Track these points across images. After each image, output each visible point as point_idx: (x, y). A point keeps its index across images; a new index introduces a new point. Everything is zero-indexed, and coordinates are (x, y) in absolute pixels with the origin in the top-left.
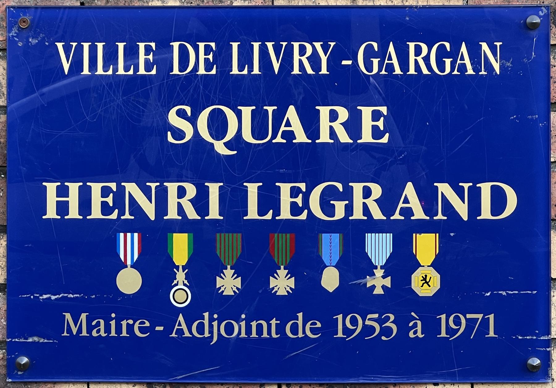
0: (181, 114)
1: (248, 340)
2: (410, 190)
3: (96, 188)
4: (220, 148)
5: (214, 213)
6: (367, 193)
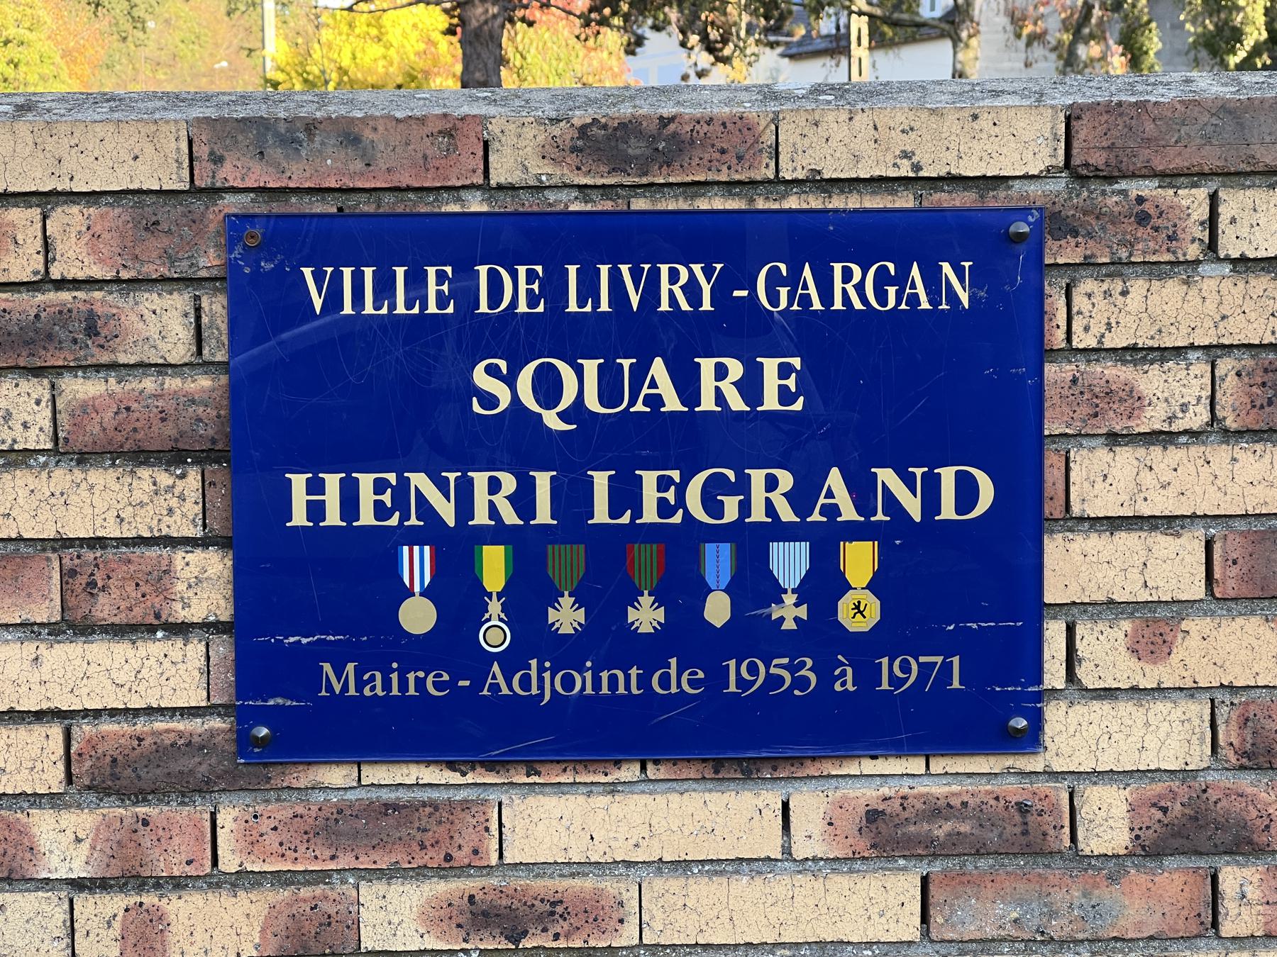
0: (492, 371)
1: (597, 698)
2: (835, 479)
3: (366, 481)
4: (552, 420)
5: (544, 515)
6: (771, 484)
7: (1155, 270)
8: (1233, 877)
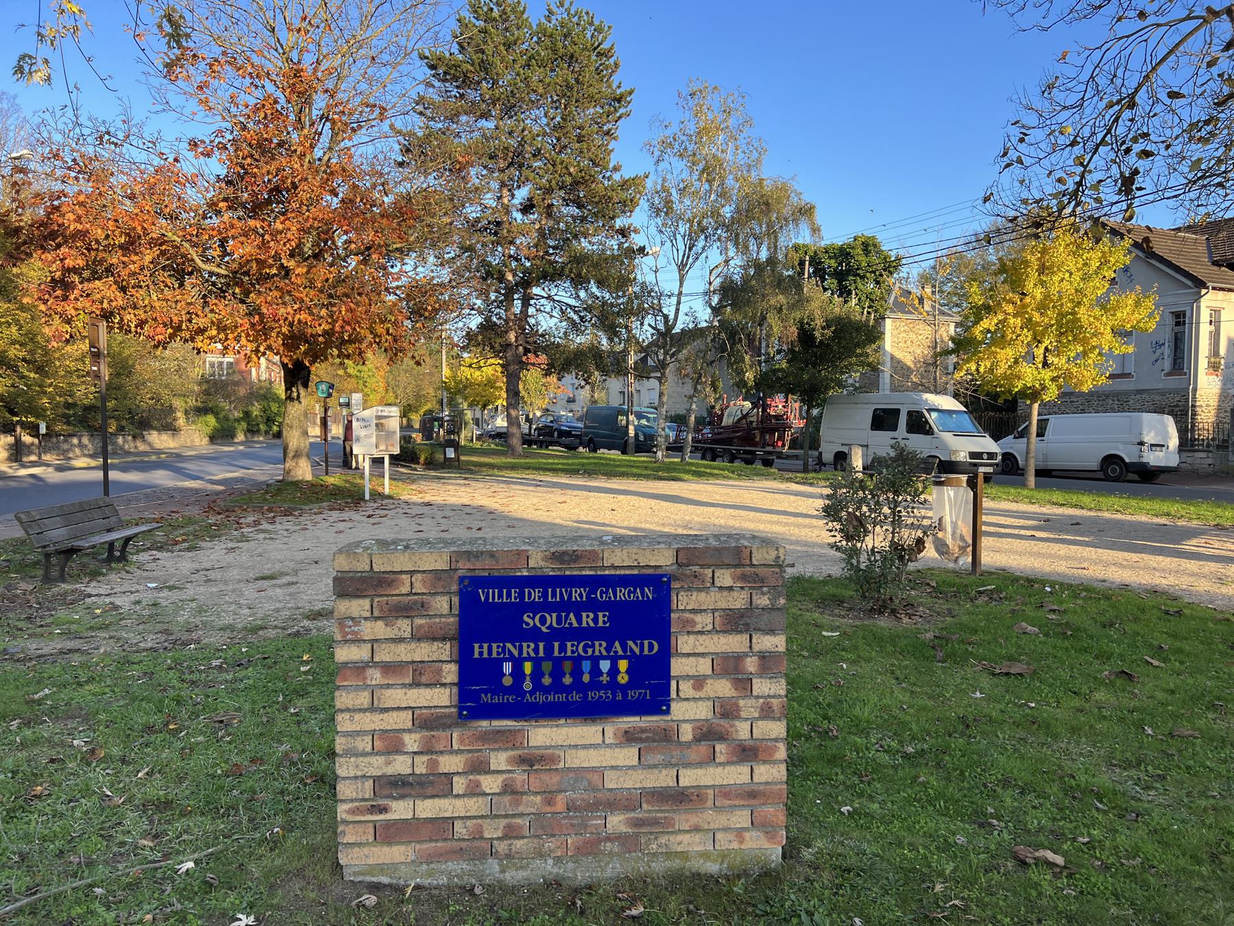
0: (529, 616)
1: (554, 702)
2: (617, 644)
3: (494, 645)
4: (544, 629)
5: (541, 654)
6: (600, 645)
7: (699, 590)
8: (719, 747)
